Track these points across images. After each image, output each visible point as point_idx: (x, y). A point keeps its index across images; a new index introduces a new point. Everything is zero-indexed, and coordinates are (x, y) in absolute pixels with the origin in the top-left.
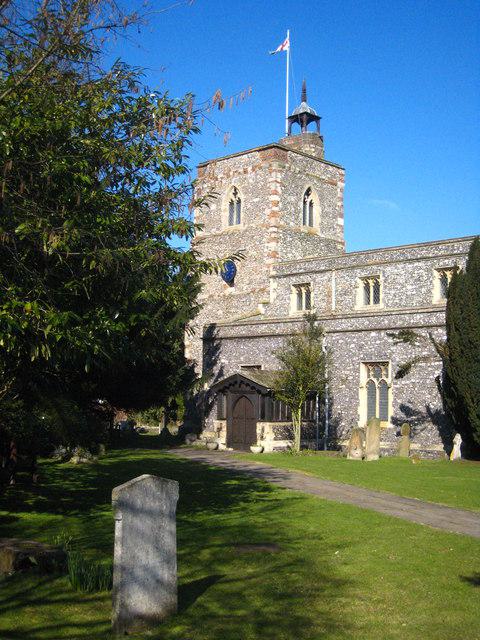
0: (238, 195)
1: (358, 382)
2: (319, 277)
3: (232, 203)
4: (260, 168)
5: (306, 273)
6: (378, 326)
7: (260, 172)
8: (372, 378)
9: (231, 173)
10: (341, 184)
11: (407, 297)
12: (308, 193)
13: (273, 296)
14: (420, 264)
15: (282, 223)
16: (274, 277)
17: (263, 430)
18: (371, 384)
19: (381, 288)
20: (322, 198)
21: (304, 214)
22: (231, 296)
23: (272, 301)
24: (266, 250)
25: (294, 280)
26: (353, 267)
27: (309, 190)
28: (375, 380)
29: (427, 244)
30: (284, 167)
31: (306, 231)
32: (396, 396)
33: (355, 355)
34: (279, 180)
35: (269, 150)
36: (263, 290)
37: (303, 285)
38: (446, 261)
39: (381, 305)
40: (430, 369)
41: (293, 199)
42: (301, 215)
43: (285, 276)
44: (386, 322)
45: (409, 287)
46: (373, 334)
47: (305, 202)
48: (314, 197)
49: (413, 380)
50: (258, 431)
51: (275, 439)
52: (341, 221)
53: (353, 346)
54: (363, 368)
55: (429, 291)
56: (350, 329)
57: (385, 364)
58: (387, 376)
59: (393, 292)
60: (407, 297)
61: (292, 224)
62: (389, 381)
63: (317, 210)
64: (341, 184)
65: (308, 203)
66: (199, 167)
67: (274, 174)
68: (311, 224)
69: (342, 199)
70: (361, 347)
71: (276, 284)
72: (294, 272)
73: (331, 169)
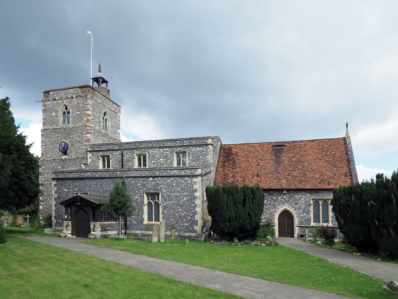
0: (68, 110)
1: (143, 202)
2: (115, 153)
3: (64, 113)
5: (108, 150)
6: (153, 175)
8: (150, 200)
11: (161, 164)
12: (105, 114)
13: (89, 160)
16: (90, 151)
17: (94, 226)
18: (149, 203)
19: (147, 159)
22: (66, 159)
23: (89, 163)
24: (84, 138)
26: (133, 149)
27: (105, 113)
28: (152, 201)
30: (93, 98)
32: (163, 209)
33: (141, 189)
36: (83, 158)
37: (106, 156)
42: (102, 124)
43: (96, 151)
45: (162, 160)
46: (151, 179)
47: (103, 119)
50: (92, 227)
51: (101, 231)
53: (139, 184)
54: (145, 195)
55: (171, 162)
57: (158, 194)
58: (158, 199)
61: (97, 127)
63: (109, 123)
66: (44, 93)
67: (88, 100)
73: (115, 105)
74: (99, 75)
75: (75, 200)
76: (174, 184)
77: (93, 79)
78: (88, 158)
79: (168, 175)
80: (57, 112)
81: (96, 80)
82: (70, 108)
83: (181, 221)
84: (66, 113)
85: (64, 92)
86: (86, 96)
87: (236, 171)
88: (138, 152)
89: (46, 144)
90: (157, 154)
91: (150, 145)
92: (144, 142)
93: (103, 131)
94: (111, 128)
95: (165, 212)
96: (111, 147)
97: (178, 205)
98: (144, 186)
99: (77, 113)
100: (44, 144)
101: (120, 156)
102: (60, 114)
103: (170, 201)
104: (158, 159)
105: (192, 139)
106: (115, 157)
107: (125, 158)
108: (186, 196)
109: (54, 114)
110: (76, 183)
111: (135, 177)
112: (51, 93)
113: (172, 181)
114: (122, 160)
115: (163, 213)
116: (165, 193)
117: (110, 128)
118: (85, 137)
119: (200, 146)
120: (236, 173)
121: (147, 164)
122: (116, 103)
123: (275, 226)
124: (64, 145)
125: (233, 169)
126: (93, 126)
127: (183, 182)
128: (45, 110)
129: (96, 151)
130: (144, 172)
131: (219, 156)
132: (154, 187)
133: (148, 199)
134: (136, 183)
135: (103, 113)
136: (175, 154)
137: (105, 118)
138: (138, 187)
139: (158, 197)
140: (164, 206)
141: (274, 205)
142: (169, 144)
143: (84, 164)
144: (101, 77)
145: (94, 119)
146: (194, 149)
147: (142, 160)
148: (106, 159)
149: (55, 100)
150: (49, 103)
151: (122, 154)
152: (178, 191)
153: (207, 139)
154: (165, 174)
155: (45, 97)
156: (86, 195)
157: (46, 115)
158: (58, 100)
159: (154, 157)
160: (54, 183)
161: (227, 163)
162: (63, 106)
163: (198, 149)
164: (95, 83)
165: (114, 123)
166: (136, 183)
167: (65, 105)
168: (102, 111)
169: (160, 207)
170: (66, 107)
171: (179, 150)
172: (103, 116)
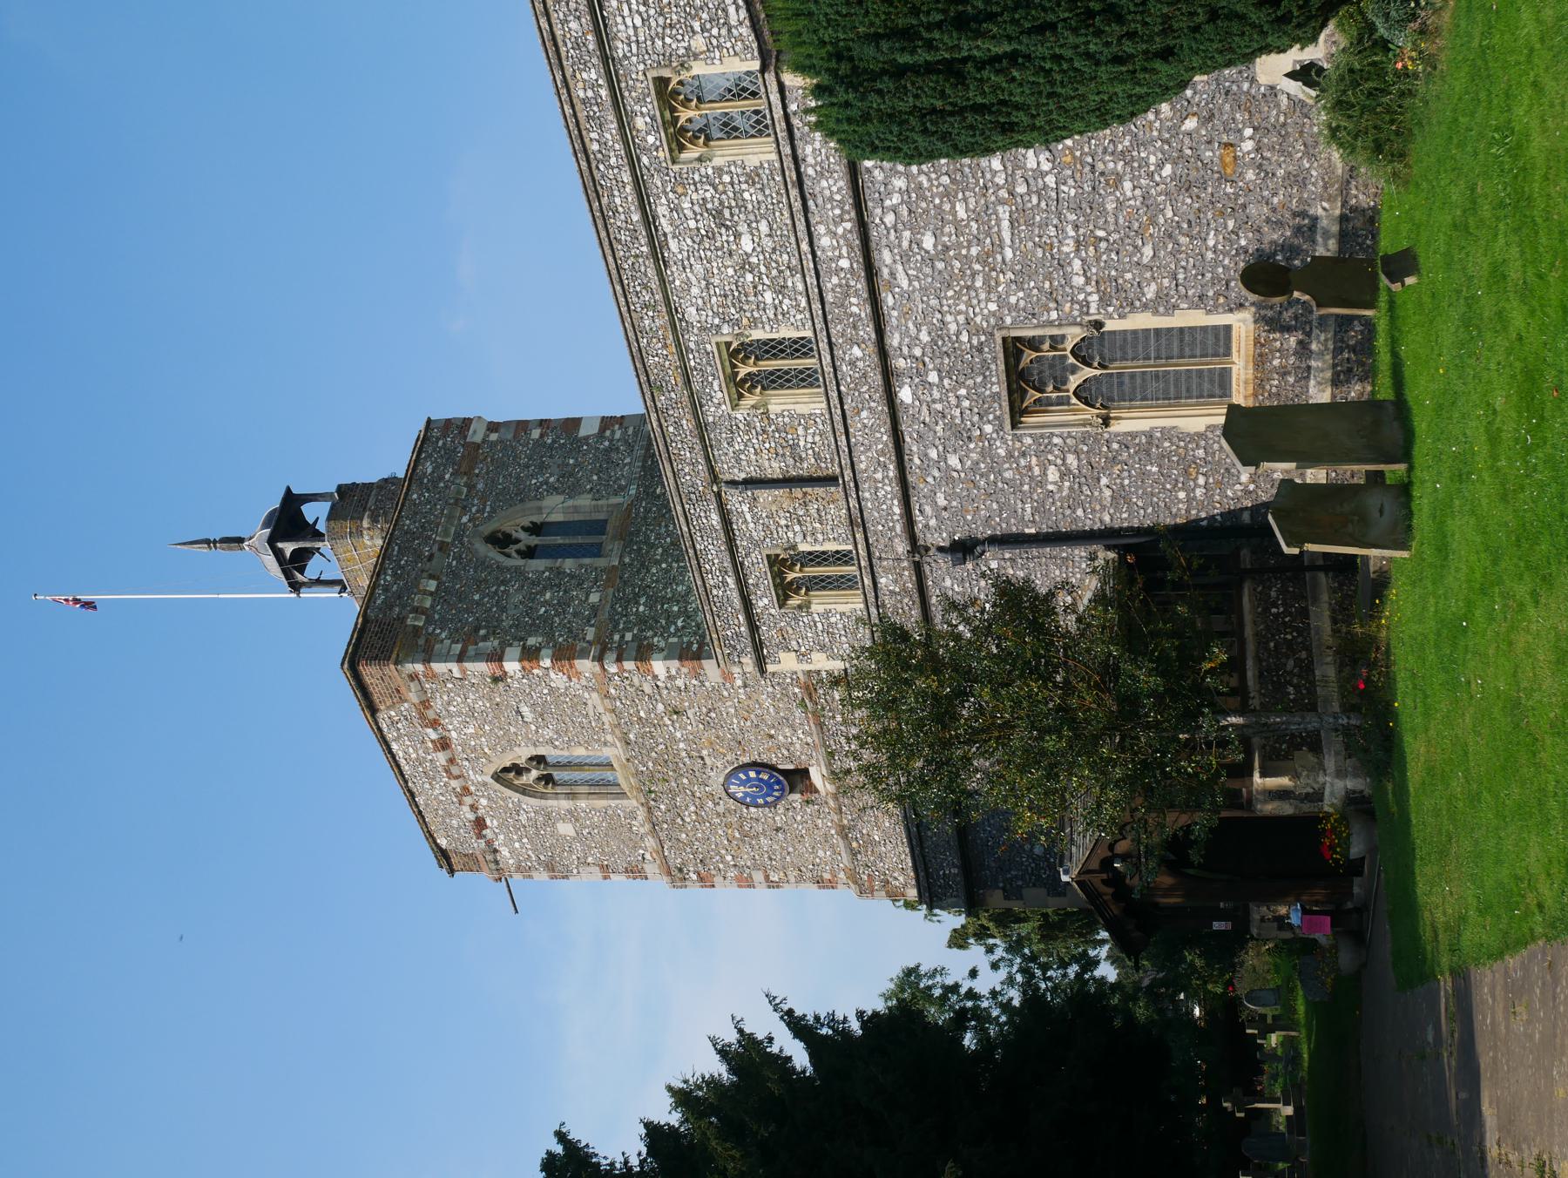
0: (522, 762)
4: (426, 704)
6: (876, 378)
7: (438, 704)
9: (454, 783)
12: (501, 541)
14: (662, 210)
15: (590, 633)
16: (761, 662)
19: (758, 334)
20: (522, 495)
24: (680, 683)
25: (764, 602)
26: (701, 428)
28: (1074, 381)
29: (593, 189)
32: (1131, 307)
34: (457, 648)
35: (368, 680)
37: (778, 576)
38: (640, 123)
40: (1021, 189)
42: (569, 565)
43: (753, 627)
44: (857, 352)
45: (747, 244)
46: (905, 394)
47: (530, 553)
48: (513, 522)
49: (1069, 247)
53: (953, 461)
56: (892, 471)
57: (1013, 348)
58: (1056, 341)
59: (768, 297)
61: (594, 598)
62: (1074, 335)
63: (555, 508)
65: (534, 540)
68: (598, 527)
70: (961, 435)
71: (782, 655)
72: (737, 602)
76: (928, 242)
78: (807, 667)
79: (861, 286)
83: (1224, 178)
88: (718, 392)
90: (708, 274)
94: (573, 491)
95: (1150, 292)
97: (1089, 207)
100: (758, 876)
101: (764, 495)
104: (745, 265)
105: (551, 43)
107: (774, 469)
109: (566, 829)
113: (905, 258)
114: (787, 482)
115: (1162, 303)
116: (1002, 302)
117: (584, 501)
118: (670, 678)
121: (795, 334)
124: (743, 783)
128: (550, 867)
129: (753, 627)
132: (959, 368)
133: (1066, 401)
134: (948, 478)
135: (493, 554)
137: (522, 535)
138: (974, 468)
139: (1034, 344)
140: (1104, 301)
142: (623, 199)
145: (546, 619)
150: (505, 852)
151: (751, 483)
152: (983, 215)
154: (858, 307)
159: (737, 297)
162: (509, 785)
165: (542, 467)
168: (483, 564)
169: (1110, 326)
170: (505, 770)
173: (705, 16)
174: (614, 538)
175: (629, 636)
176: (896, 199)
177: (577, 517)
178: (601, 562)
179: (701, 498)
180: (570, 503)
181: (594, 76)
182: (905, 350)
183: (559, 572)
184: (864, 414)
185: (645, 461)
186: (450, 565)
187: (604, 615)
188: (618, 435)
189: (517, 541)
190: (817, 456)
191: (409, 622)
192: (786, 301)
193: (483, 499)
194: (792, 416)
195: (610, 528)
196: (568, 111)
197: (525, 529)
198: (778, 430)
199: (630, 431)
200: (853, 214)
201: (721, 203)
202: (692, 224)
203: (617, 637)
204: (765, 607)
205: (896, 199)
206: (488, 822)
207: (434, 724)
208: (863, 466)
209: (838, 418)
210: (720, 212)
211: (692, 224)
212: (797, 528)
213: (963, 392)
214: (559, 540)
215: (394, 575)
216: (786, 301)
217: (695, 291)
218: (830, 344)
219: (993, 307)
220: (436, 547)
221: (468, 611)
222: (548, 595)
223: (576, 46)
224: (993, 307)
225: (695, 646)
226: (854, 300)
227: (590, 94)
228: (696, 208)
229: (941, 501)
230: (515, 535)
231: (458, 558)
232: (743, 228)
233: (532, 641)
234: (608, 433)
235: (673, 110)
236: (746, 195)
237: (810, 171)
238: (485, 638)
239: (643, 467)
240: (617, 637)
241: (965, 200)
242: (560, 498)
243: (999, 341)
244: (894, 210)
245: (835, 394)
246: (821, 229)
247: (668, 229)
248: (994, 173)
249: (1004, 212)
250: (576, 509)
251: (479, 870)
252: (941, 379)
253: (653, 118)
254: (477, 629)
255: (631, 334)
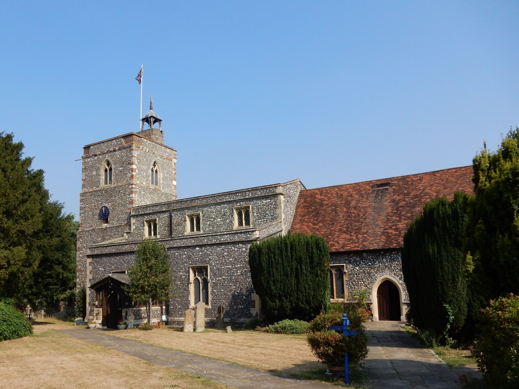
2: (162, 216)
3: (106, 170)
7: (123, 150)
10: (175, 161)
11: (218, 226)
12: (155, 164)
19: (201, 220)
21: (152, 178)
27: (155, 163)
30: (139, 148)
31: (153, 188)
39: (202, 232)
41: (145, 168)
42: (150, 178)
44: (205, 241)
46: (197, 249)
47: (152, 170)
52: (175, 183)
55: (231, 222)
57: (206, 268)
60: (218, 226)
61: (144, 183)
63: (160, 175)
64: (175, 161)
68: (156, 184)
69: (175, 170)
72: (146, 212)
73: (168, 150)
74: (150, 113)
75: (106, 282)
76: (225, 254)
77: (143, 120)
79: (218, 242)
80: (98, 169)
81: (146, 120)
82: (112, 164)
84: (109, 171)
85: (106, 144)
86: (130, 146)
87: (317, 227)
89: (85, 211)
91: (204, 202)
92: (197, 198)
93: (152, 187)
94: (163, 180)
96: (157, 209)
98: (189, 258)
99: (120, 169)
101: (167, 219)
102: (102, 172)
103: (221, 276)
106: (162, 221)
107: (174, 221)
108: (240, 268)
110: (112, 259)
111: (179, 248)
112: (91, 147)
116: (214, 266)
119: (266, 197)
120: (318, 229)
122: (170, 146)
123: (371, 304)
125: (314, 224)
126: (138, 182)
127: (236, 250)
130: (189, 240)
131: (297, 207)
134: (180, 255)
135: (153, 163)
136: (235, 211)
137: (155, 169)
141: (369, 273)
142: (228, 199)
143: (128, 233)
144: (152, 116)
146: (259, 202)
147: (196, 221)
148: (153, 225)
149: (96, 155)
151: (171, 216)
152: (231, 263)
153: (276, 187)
154: (214, 241)
155: (85, 153)
156: (122, 275)
157: (86, 175)
158: (99, 155)
159: (209, 217)
160: (89, 260)
161: (307, 217)
163: (265, 201)
164: (145, 123)
166: (180, 255)
167: (107, 160)
168: (151, 161)
171: (241, 205)
172: (152, 167)
173: (260, 216)
174: (155, 187)
175: (138, 190)
176: (233, 249)
177: (158, 180)
178: (151, 184)
179: (169, 207)
180: (161, 179)
181: (250, 195)
182: (206, 249)
183: (149, 176)
184: (194, 241)
185: (168, 194)
186: (151, 154)
187: (141, 185)
188: (173, 188)
189: (154, 168)
190: (177, 229)
191: (141, 146)
192: (207, 226)
193: (162, 161)
194: (185, 225)
195: (156, 186)
196: (244, 190)
197: (157, 169)
198: (182, 223)
199: (173, 191)
200: (231, 241)
201: (226, 216)
202: (223, 210)
203: (138, 187)
204: (145, 217)
205: (233, 249)
206: (96, 157)
207: (119, 149)
208: (184, 240)
209: (193, 236)
210: (225, 215)
211: (223, 210)
212: (162, 225)
213: (198, 259)
214: (154, 176)
215: (149, 143)
216: (207, 226)
217: (210, 210)
218: (208, 236)
219: (213, 264)
220: (154, 152)
221: (142, 158)
222: (145, 174)
223: (256, 193)
224: (213, 264)
225: (135, 203)
226: (215, 240)
227: (247, 194)
228: (225, 211)
229: (177, 254)
230: (155, 167)
231: (152, 156)
232: (222, 219)
233: (137, 170)
234: (173, 186)
235: (244, 209)
236: (227, 220)
237: (239, 235)
238: (138, 161)
239: (167, 193)
240: (138, 187)
241: (233, 260)
242: (162, 177)
243: (207, 265)
244: (232, 248)
245: (198, 236)
246: (228, 236)
247: (222, 206)
248: (237, 265)
249: (230, 266)
250: (160, 180)
251: (85, 154)
252: (200, 255)
253: (242, 205)
254: (139, 160)
255: (202, 197)
